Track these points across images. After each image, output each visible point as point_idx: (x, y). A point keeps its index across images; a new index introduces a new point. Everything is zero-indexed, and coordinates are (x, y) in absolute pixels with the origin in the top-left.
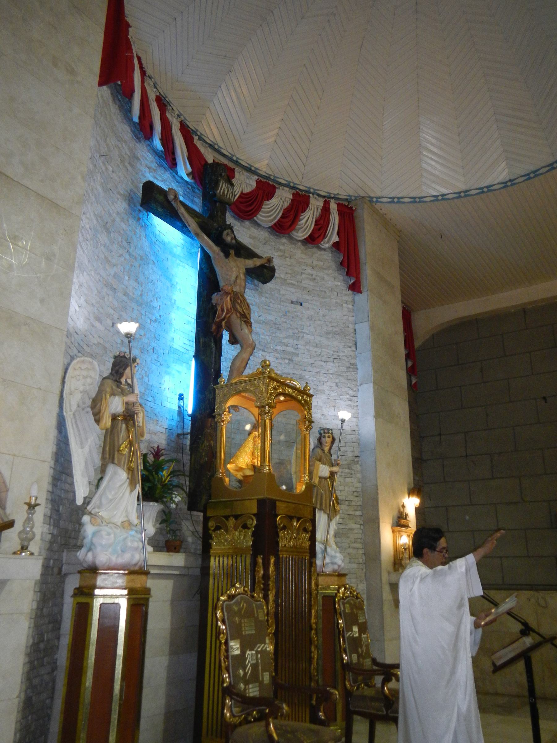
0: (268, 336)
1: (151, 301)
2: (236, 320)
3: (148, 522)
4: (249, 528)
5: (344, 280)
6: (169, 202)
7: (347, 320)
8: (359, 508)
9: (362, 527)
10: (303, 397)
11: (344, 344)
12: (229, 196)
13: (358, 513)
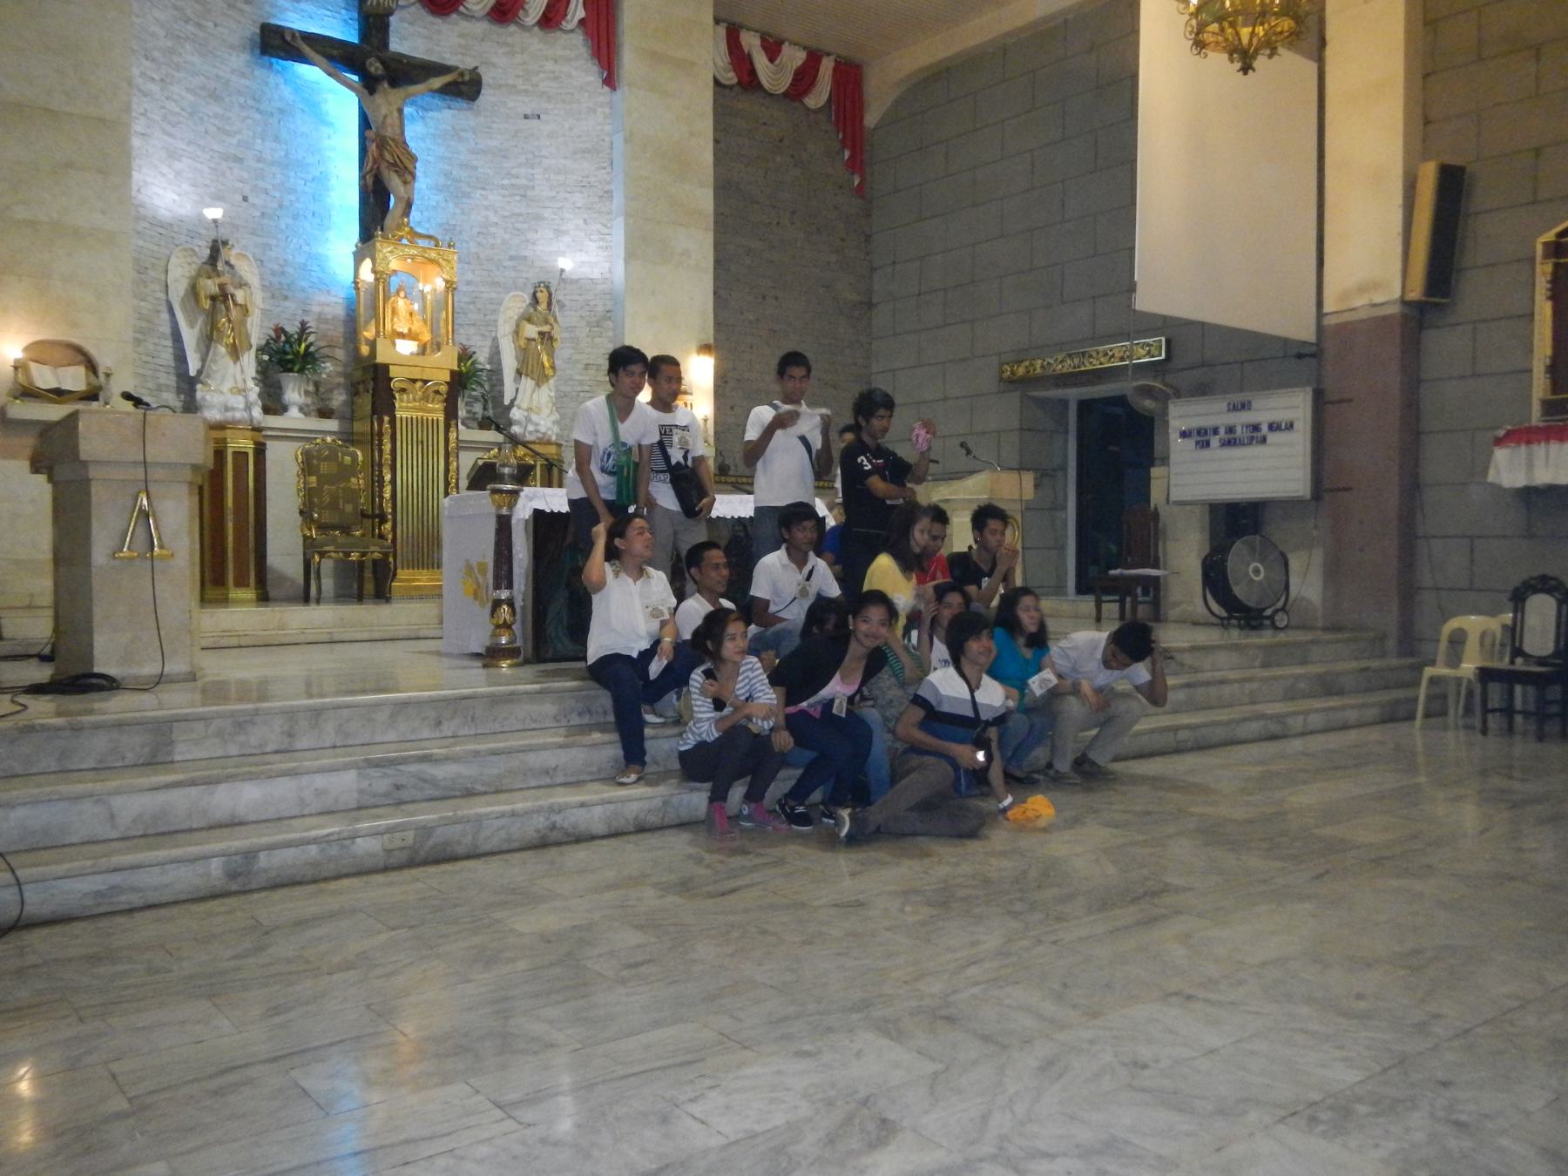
0: (490, 168)
1: (304, 158)
3: (293, 391)
6: (288, 43)
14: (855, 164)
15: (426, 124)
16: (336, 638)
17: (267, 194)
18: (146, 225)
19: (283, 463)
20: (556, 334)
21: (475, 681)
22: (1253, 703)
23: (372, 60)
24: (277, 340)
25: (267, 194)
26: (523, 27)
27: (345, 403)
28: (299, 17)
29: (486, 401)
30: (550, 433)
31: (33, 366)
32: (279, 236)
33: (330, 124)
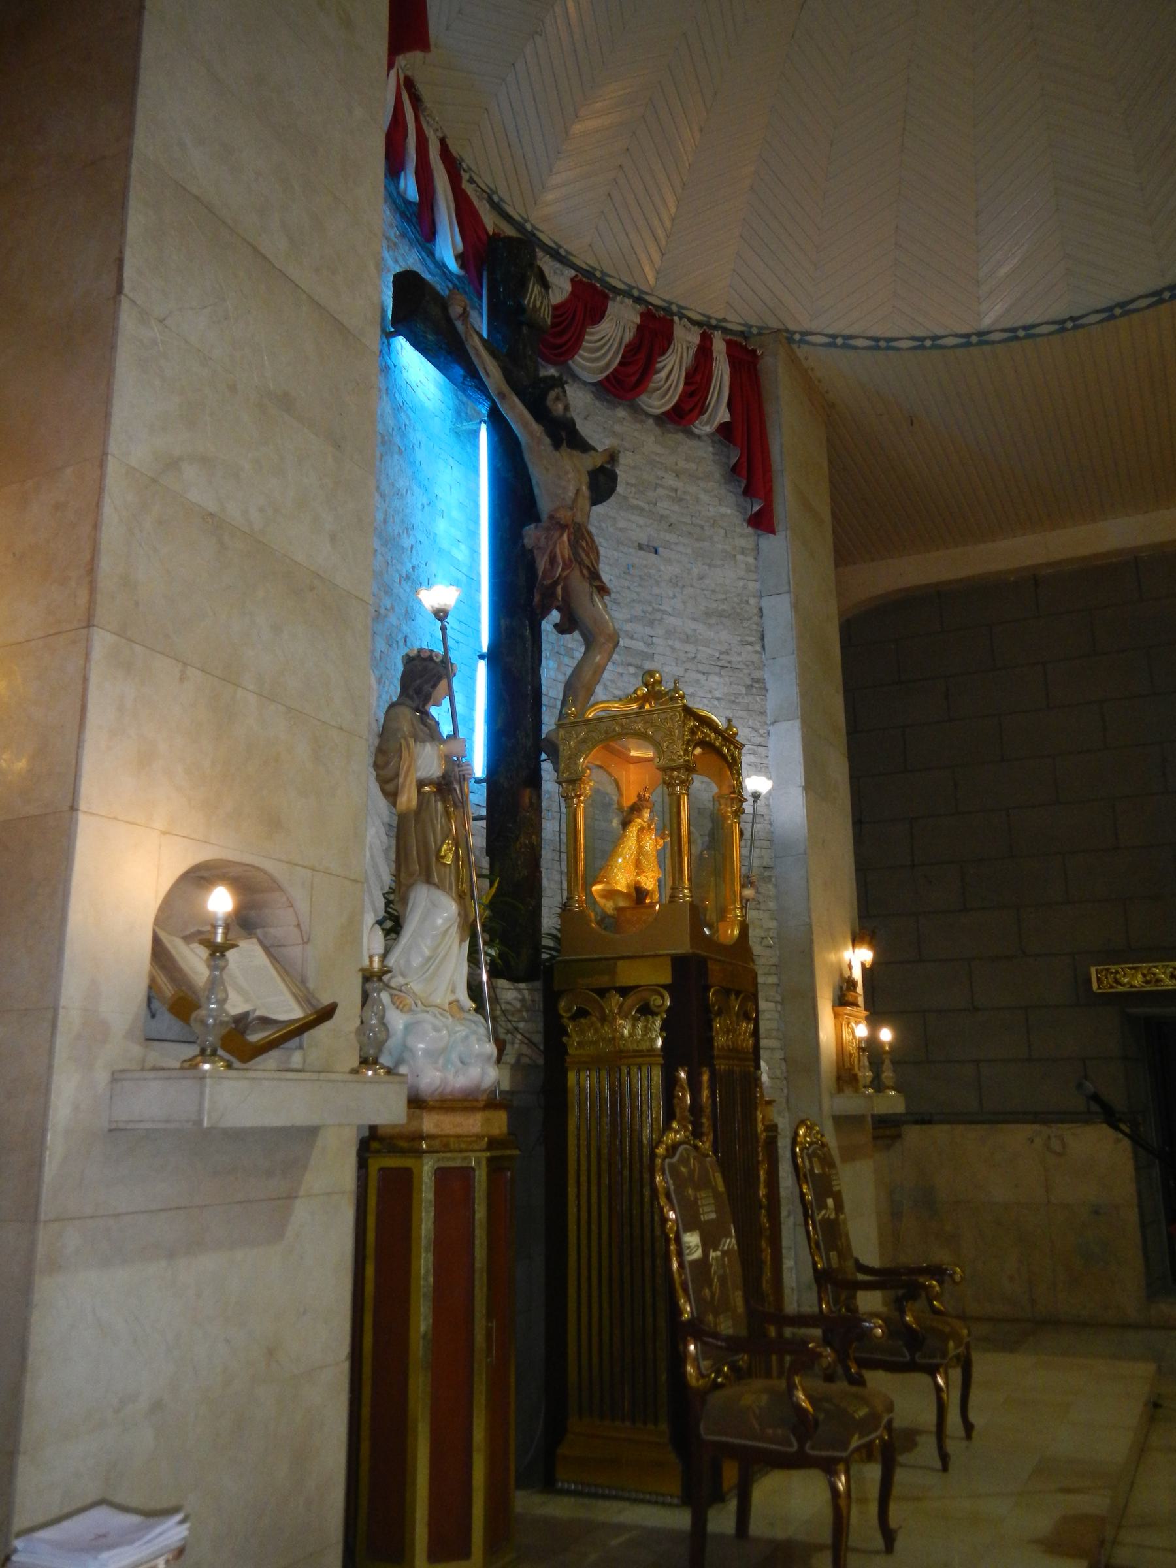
2: (579, 585)
4: (654, 1014)
5: (738, 505)
6: (449, 320)
7: (745, 587)
8: (773, 970)
9: (779, 1008)
10: (729, 750)
11: (739, 638)
12: (544, 314)
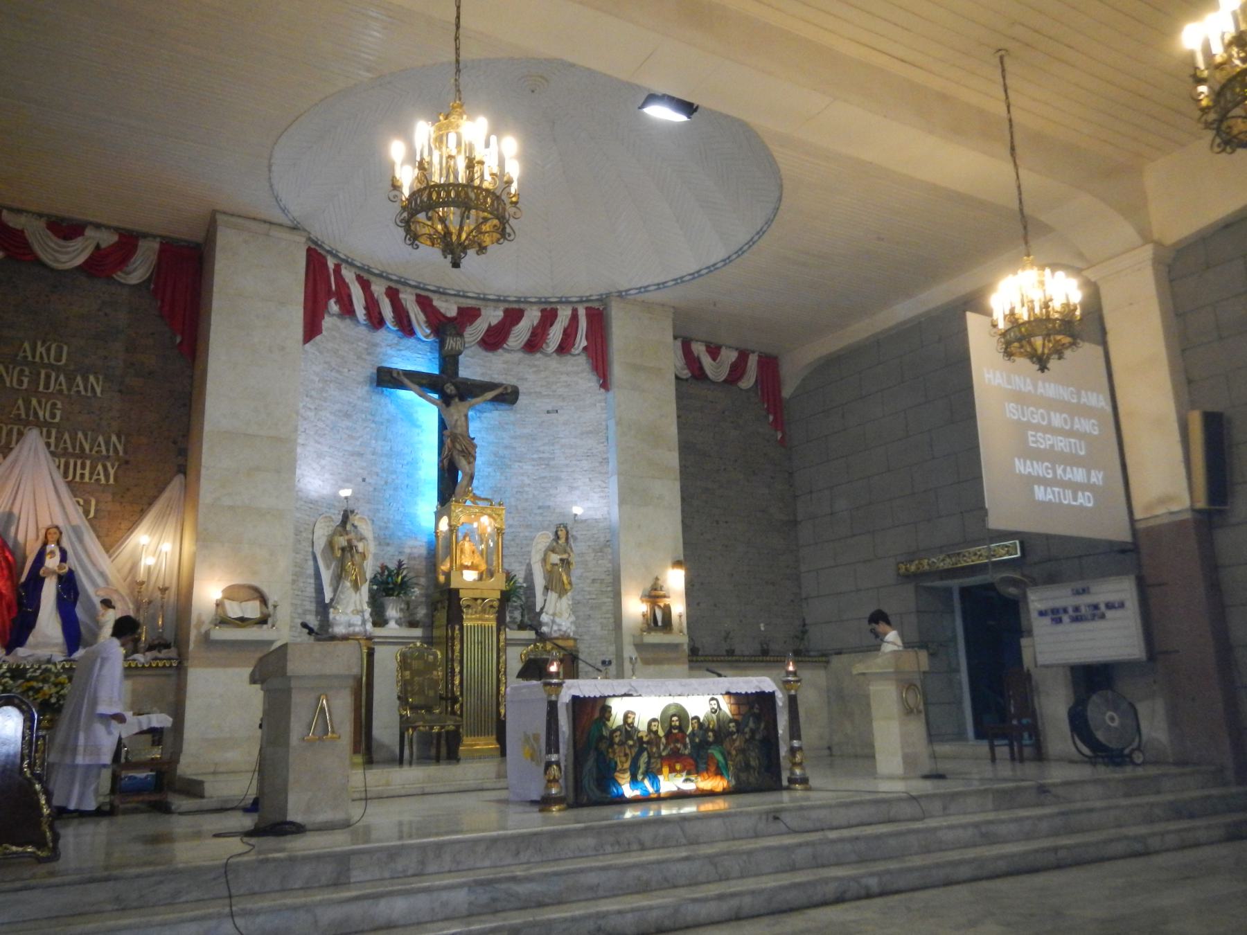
3: (392, 609)
13: (609, 589)
14: (778, 424)
15: (481, 421)
16: (427, 790)
17: (378, 475)
18: (302, 503)
19: (387, 660)
20: (573, 559)
21: (531, 822)
22: (1120, 826)
23: (448, 385)
24: (382, 574)
25: (378, 475)
26: (547, 355)
27: (426, 615)
28: (400, 360)
29: (523, 610)
30: (569, 631)
31: (227, 602)
32: (385, 503)
33: (419, 427)
